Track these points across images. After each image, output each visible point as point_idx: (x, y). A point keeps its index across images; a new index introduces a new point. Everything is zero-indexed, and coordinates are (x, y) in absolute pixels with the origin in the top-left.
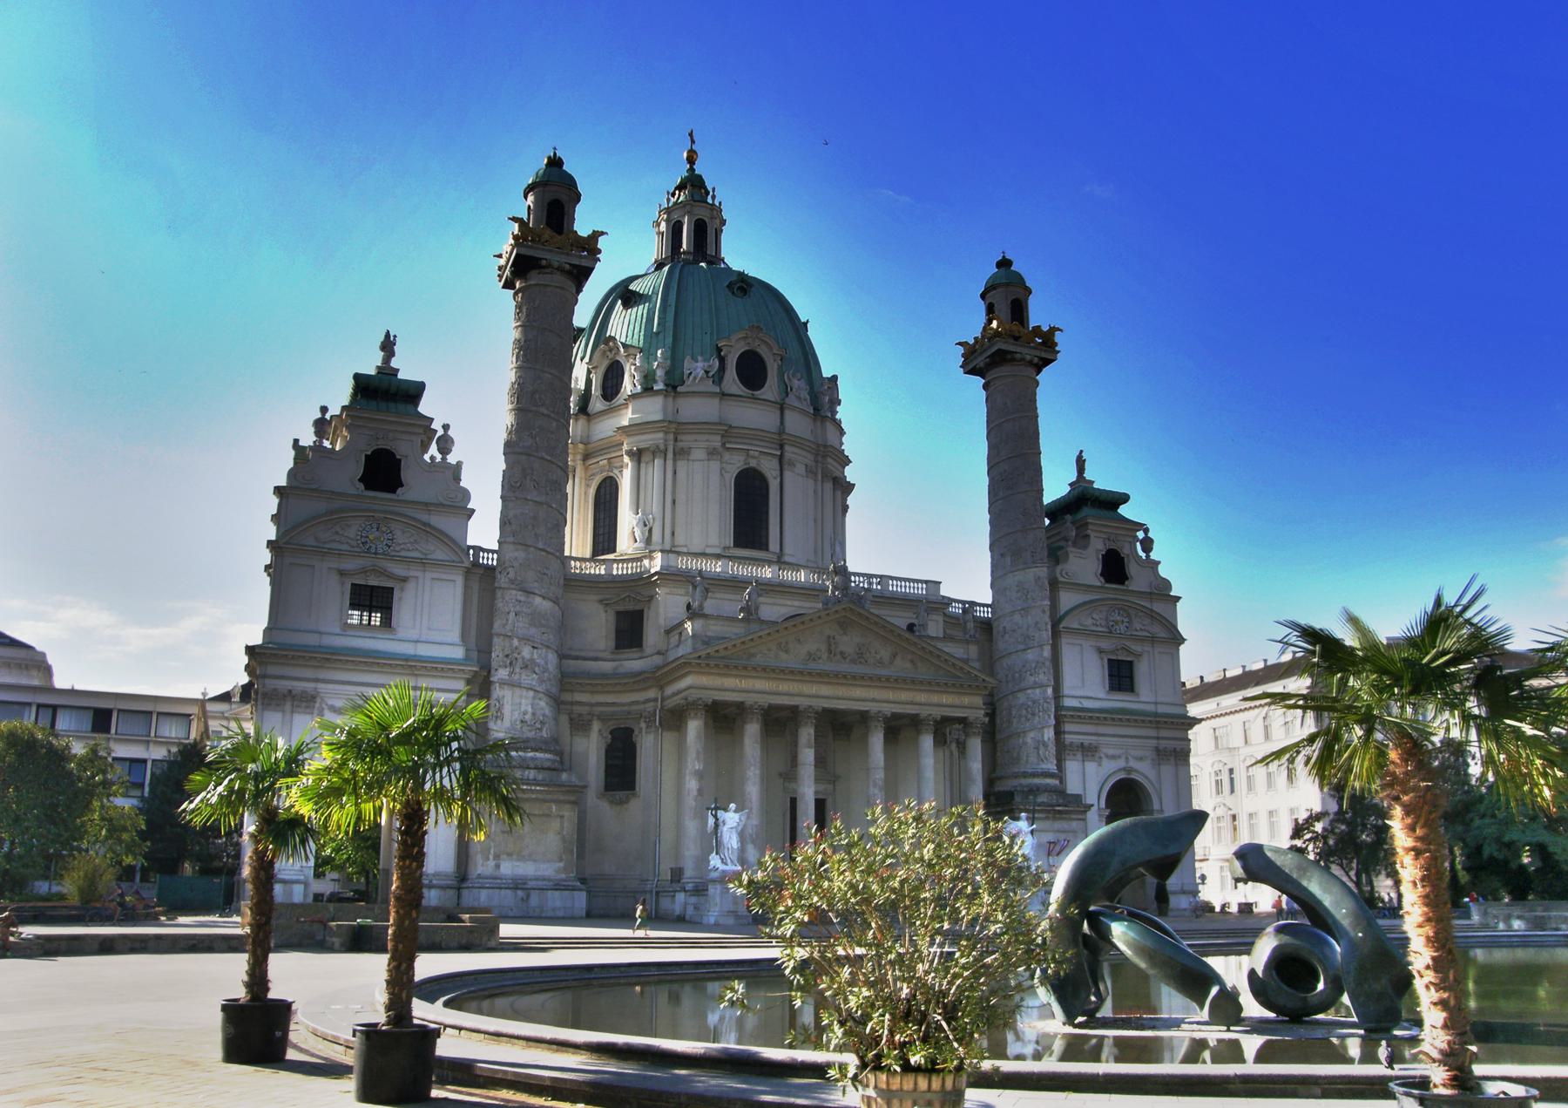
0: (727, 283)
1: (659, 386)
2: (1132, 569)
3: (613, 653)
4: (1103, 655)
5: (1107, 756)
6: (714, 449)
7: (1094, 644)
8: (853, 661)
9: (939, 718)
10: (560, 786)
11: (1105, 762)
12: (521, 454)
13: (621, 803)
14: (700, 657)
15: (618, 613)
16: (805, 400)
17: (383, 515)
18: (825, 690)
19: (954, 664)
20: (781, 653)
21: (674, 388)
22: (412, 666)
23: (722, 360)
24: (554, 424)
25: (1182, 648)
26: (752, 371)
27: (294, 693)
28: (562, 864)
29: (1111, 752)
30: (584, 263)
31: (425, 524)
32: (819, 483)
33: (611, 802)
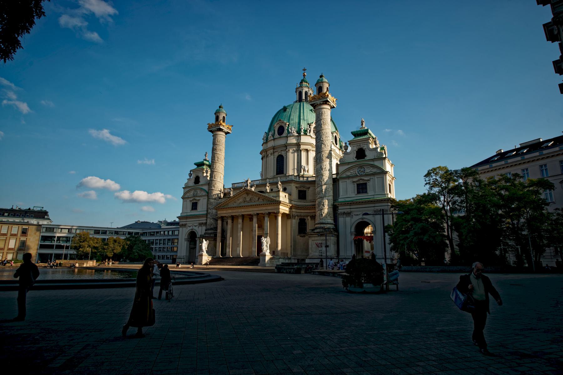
2: (367, 153)
4: (354, 183)
5: (355, 215)
6: (272, 153)
7: (351, 180)
8: (248, 202)
11: (354, 216)
14: (217, 207)
17: (195, 189)
18: (243, 210)
20: (234, 203)
23: (274, 130)
26: (281, 130)
28: (211, 253)
29: (356, 213)
30: (218, 127)
32: (299, 153)
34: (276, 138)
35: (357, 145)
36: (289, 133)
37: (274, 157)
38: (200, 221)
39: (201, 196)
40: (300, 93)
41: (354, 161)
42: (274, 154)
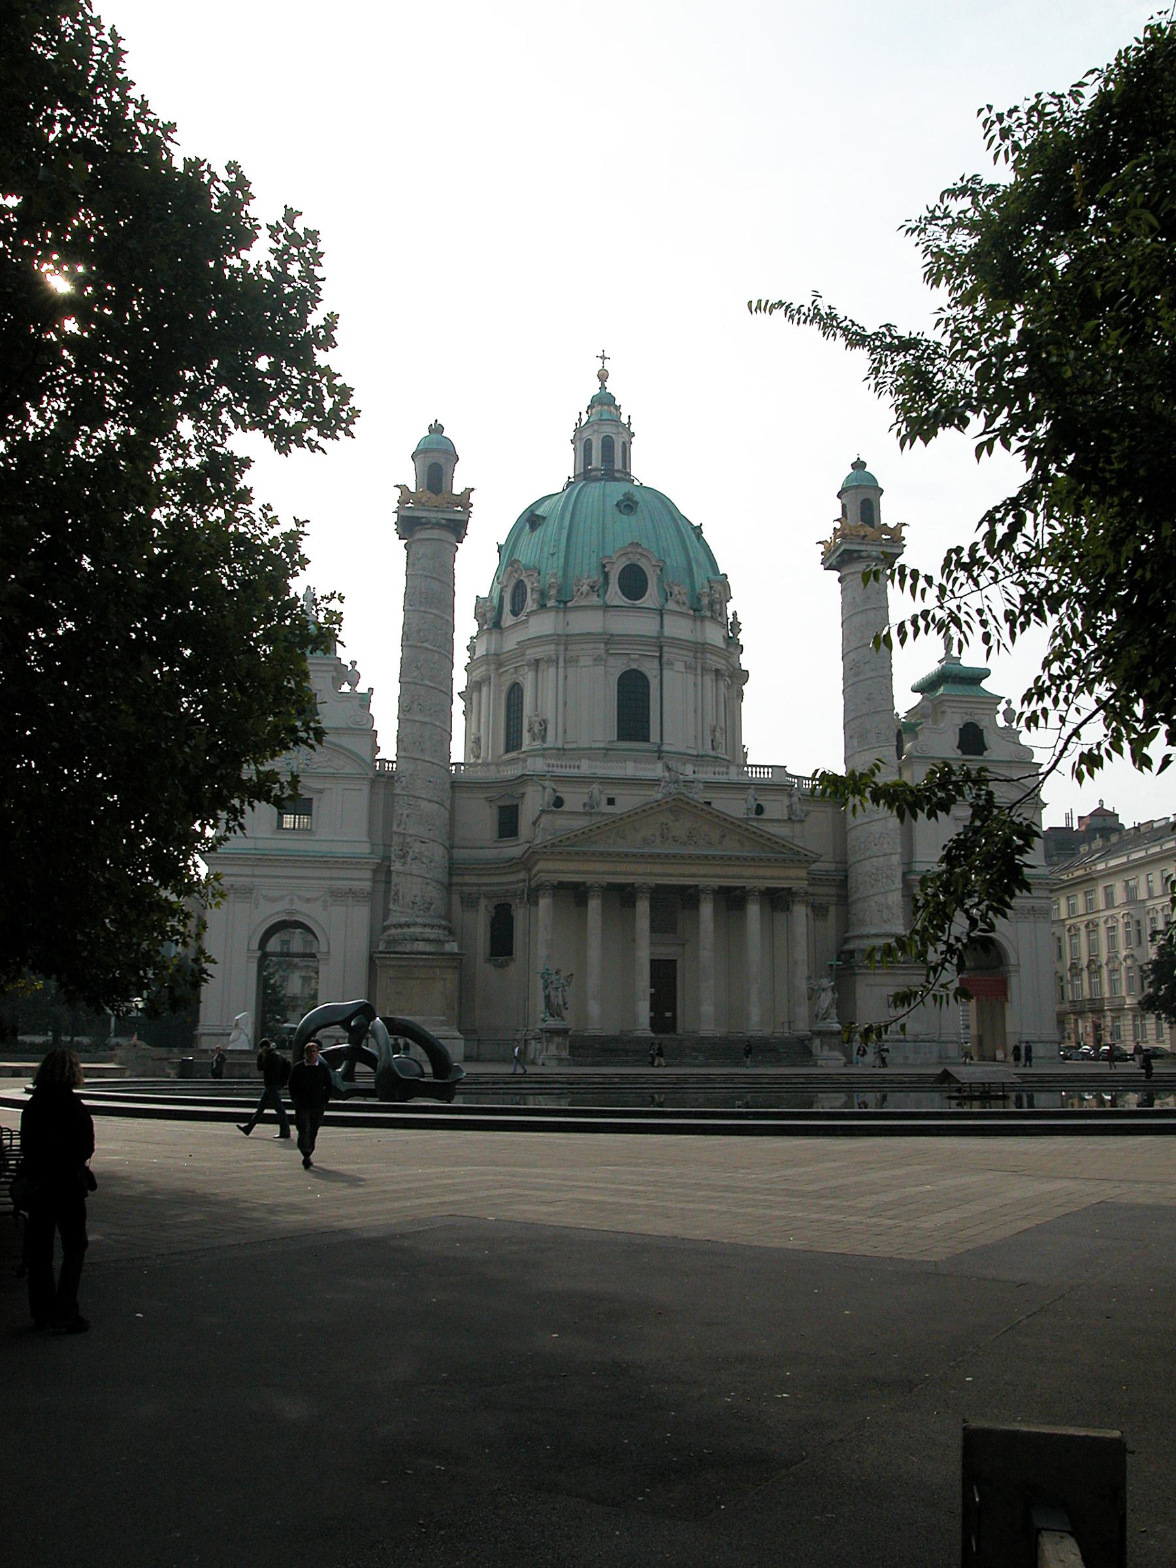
0: (615, 502)
1: (551, 603)
2: (989, 739)
3: (495, 841)
4: (958, 822)
9: (763, 889)
10: (443, 954)
12: (410, 683)
13: (502, 966)
14: (545, 847)
15: (502, 809)
16: (684, 604)
18: (658, 869)
19: (776, 842)
21: (565, 603)
22: (324, 861)
23: (606, 576)
24: (437, 656)
25: (1043, 811)
27: (235, 887)
28: (444, 1018)
30: (458, 517)
31: (335, 745)
32: (700, 677)
33: (495, 966)
34: (612, 604)
35: (964, 710)
36: (667, 600)
37: (606, 676)
38: (333, 882)
39: (333, 776)
40: (608, 445)
41: (956, 756)
42: (605, 661)
